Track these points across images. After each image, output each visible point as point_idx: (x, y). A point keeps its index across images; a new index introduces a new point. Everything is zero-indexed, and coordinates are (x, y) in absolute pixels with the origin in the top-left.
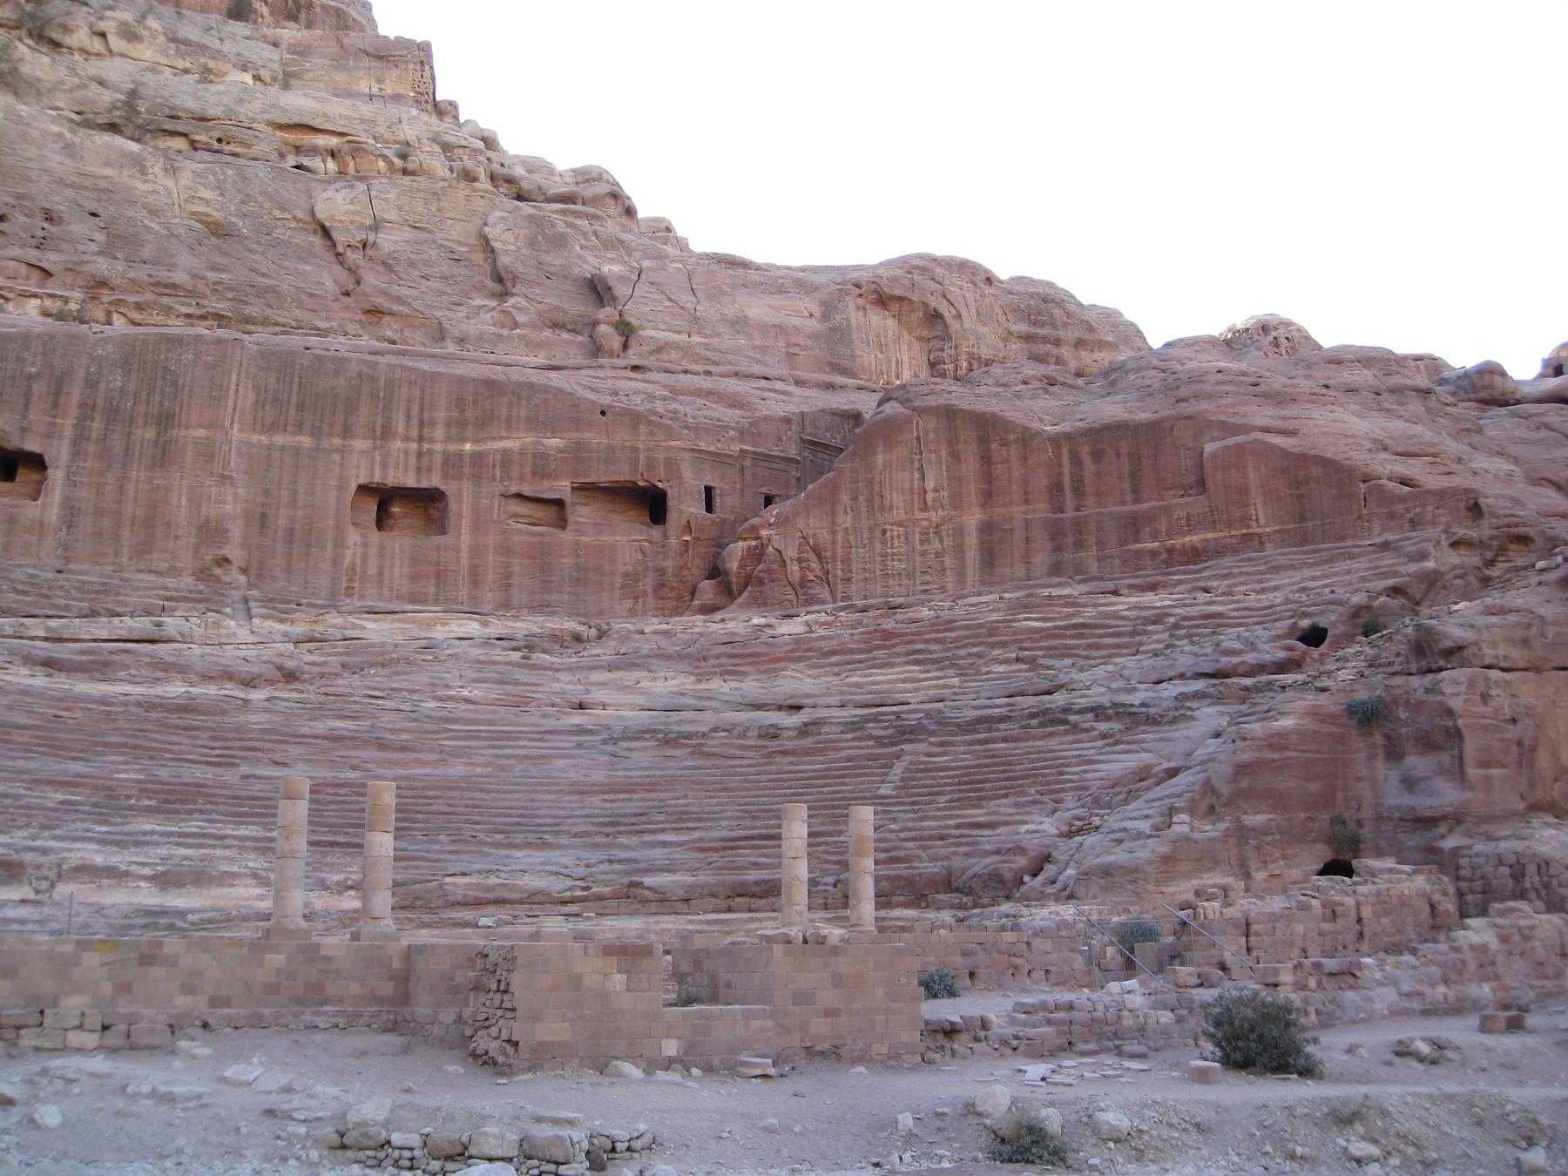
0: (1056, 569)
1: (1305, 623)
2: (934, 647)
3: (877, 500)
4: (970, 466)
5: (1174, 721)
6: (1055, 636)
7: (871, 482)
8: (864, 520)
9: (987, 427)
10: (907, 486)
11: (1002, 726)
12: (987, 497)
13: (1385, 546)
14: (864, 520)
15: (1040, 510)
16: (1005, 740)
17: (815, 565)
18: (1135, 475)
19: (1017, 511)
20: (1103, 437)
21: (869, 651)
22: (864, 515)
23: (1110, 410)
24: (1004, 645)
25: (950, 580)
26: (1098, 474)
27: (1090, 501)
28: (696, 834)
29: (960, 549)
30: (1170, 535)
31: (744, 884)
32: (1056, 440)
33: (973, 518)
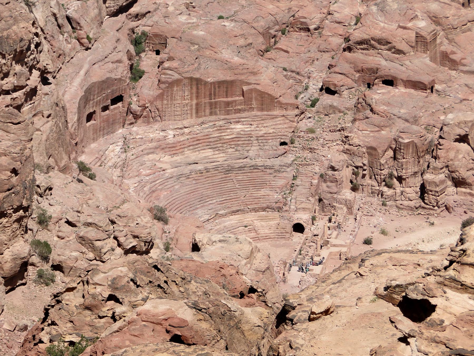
0: (211, 114)
1: (282, 141)
2: (211, 144)
3: (173, 98)
4: (194, 90)
5: (283, 172)
6: (233, 141)
7: (172, 93)
8: (169, 102)
9: (198, 81)
10: (181, 95)
11: (246, 168)
12: (197, 97)
13: (283, 116)
14: (169, 102)
15: (207, 100)
16: (249, 173)
17: (157, 112)
18: (227, 92)
19: (203, 100)
20: (221, 83)
21: (197, 144)
22: (170, 101)
23: (221, 76)
24: (225, 143)
25: (189, 115)
26: (219, 91)
27: (217, 97)
28: (215, 201)
29: (191, 109)
30: (235, 107)
31: (234, 211)
32: (211, 83)
33: (194, 102)
